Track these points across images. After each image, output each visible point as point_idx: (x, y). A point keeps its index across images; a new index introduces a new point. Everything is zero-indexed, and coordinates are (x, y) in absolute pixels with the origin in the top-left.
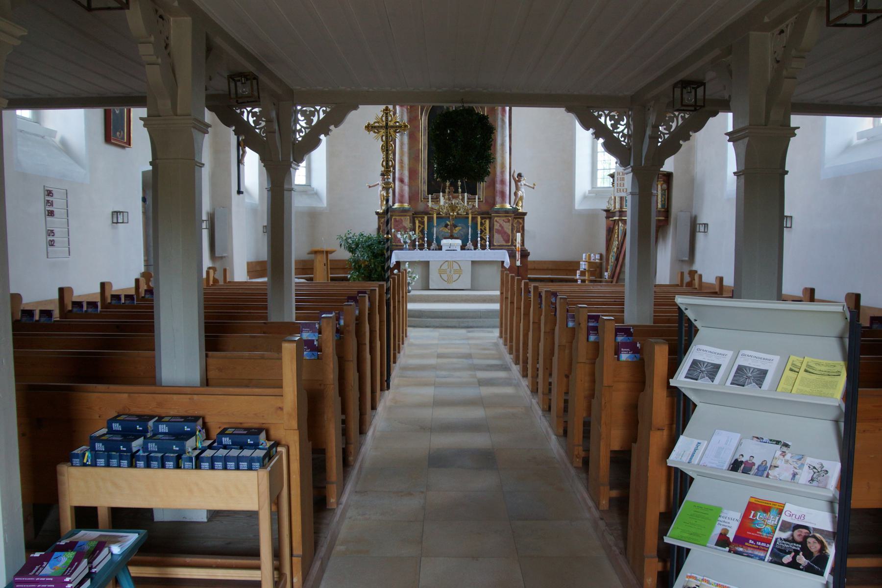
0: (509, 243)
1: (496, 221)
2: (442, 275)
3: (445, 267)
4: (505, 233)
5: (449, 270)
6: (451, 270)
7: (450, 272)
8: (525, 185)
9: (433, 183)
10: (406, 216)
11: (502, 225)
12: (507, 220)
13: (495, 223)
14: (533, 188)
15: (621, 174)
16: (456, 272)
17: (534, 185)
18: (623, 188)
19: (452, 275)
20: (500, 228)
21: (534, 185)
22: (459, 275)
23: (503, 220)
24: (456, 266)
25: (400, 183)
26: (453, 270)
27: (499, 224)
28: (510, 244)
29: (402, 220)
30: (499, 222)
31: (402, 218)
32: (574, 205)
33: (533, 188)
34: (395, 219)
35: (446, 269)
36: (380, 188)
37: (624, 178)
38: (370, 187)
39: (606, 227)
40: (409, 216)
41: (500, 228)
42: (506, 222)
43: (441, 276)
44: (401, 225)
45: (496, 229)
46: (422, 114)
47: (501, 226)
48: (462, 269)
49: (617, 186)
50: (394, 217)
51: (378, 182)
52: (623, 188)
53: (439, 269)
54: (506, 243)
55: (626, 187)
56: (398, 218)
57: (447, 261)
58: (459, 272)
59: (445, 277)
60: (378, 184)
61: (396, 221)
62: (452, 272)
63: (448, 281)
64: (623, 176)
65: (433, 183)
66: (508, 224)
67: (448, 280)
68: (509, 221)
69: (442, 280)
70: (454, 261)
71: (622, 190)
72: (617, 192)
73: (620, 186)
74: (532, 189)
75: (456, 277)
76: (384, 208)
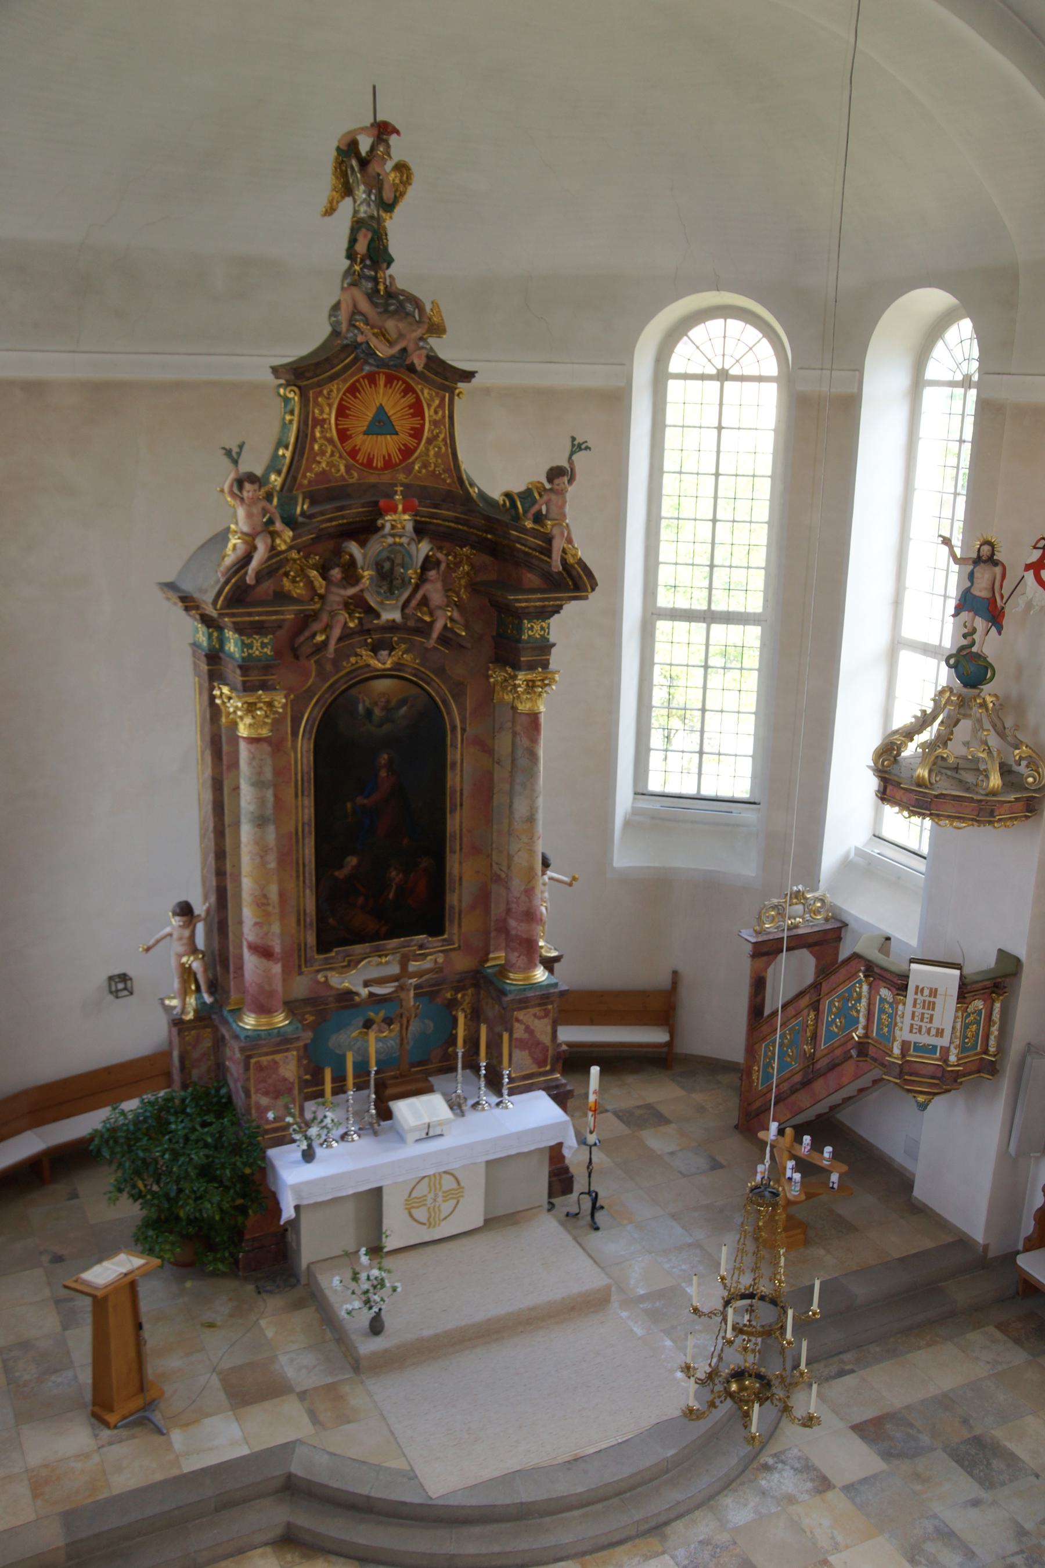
0: (546, 1066)
1: (517, 1020)
2: (413, 1211)
3: (422, 1189)
4: (538, 1043)
5: (432, 1195)
6: (436, 1196)
7: (435, 1200)
8: (551, 879)
9: (331, 920)
10: (287, 1050)
11: (532, 1027)
12: (542, 1014)
13: (516, 1025)
14: (570, 885)
15: (926, 992)
16: (448, 1195)
17: (574, 879)
18: (929, 1026)
19: (439, 1206)
20: (526, 1036)
21: (574, 879)
22: (455, 1201)
23: (535, 1015)
24: (448, 1183)
25: (264, 960)
26: (440, 1194)
27: (523, 1027)
28: (548, 1068)
29: (276, 1062)
30: (525, 1021)
31: (278, 1057)
32: (612, 859)
33: (570, 885)
34: (258, 1062)
35: (425, 1196)
36: (178, 947)
37: (934, 1003)
38: (148, 949)
39: (751, 978)
40: (297, 1049)
41: (526, 1036)
42: (540, 1018)
43: (411, 1216)
44: (274, 1076)
45: (516, 1039)
46: (295, 734)
47: (528, 1030)
48: (462, 1184)
49: (913, 1018)
50: (253, 1061)
51: (168, 930)
52: (929, 1026)
53: (406, 1200)
54: (540, 1067)
55: (936, 1023)
56: (265, 1060)
57: (424, 1177)
58: (457, 1194)
59: (421, 1214)
60: (170, 935)
61: (260, 1068)
62: (440, 1199)
63: (430, 1224)
64: (932, 999)
65: (331, 920)
66: (546, 1021)
67: (429, 1219)
68: (546, 1016)
69: (415, 1224)
70: (445, 1172)
71: (924, 1030)
72: (911, 1031)
73: (922, 1020)
74: (567, 886)
75: (446, 1207)
76: (192, 1001)
